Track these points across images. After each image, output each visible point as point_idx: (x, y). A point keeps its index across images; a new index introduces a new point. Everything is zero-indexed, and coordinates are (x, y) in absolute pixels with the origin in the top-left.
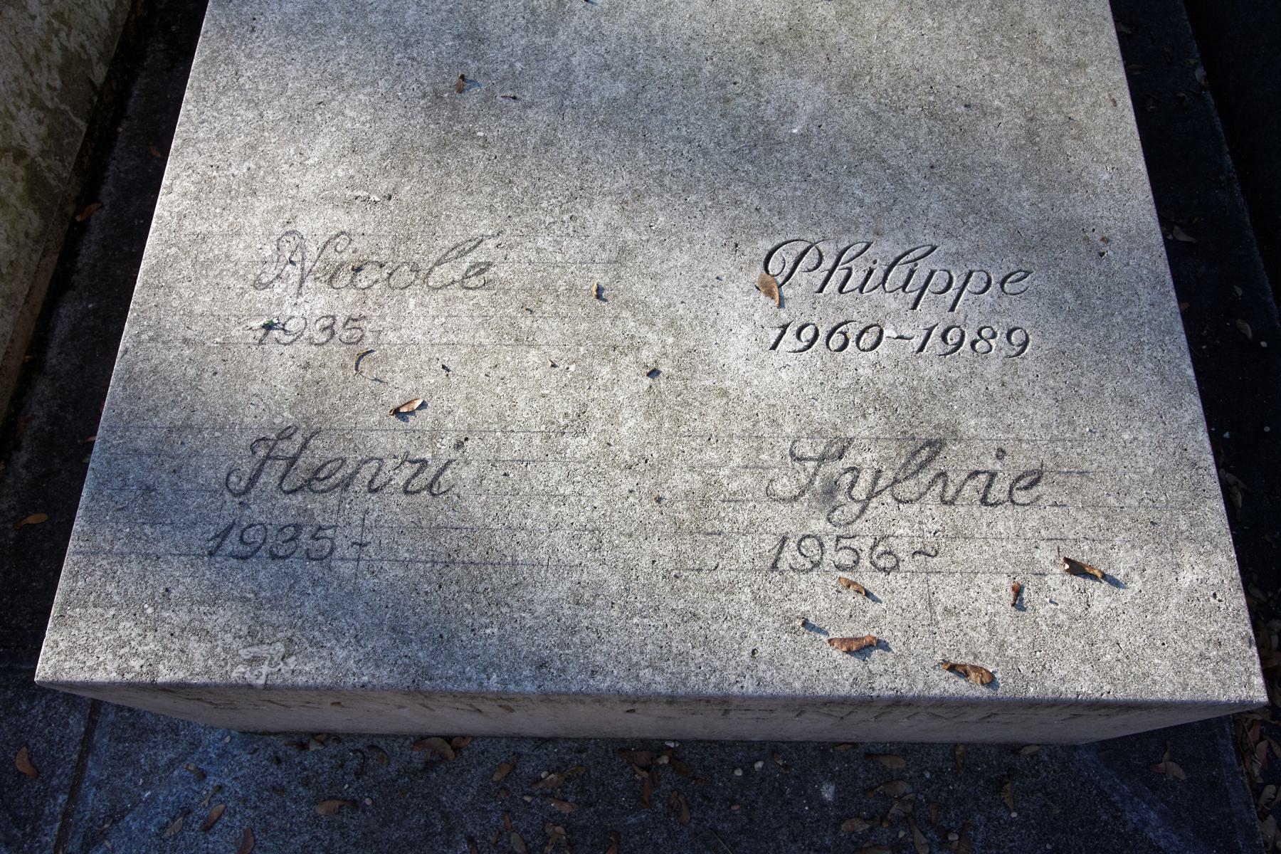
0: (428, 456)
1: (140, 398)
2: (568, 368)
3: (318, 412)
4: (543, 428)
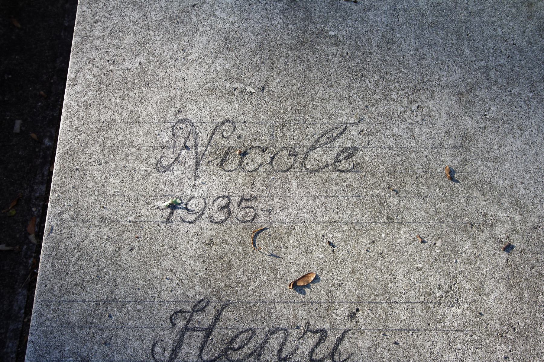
0: (326, 326)
1: (67, 274)
2: (435, 244)
3: (226, 285)
4: (422, 298)
